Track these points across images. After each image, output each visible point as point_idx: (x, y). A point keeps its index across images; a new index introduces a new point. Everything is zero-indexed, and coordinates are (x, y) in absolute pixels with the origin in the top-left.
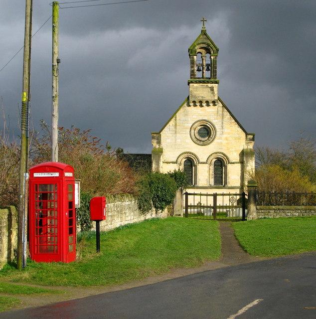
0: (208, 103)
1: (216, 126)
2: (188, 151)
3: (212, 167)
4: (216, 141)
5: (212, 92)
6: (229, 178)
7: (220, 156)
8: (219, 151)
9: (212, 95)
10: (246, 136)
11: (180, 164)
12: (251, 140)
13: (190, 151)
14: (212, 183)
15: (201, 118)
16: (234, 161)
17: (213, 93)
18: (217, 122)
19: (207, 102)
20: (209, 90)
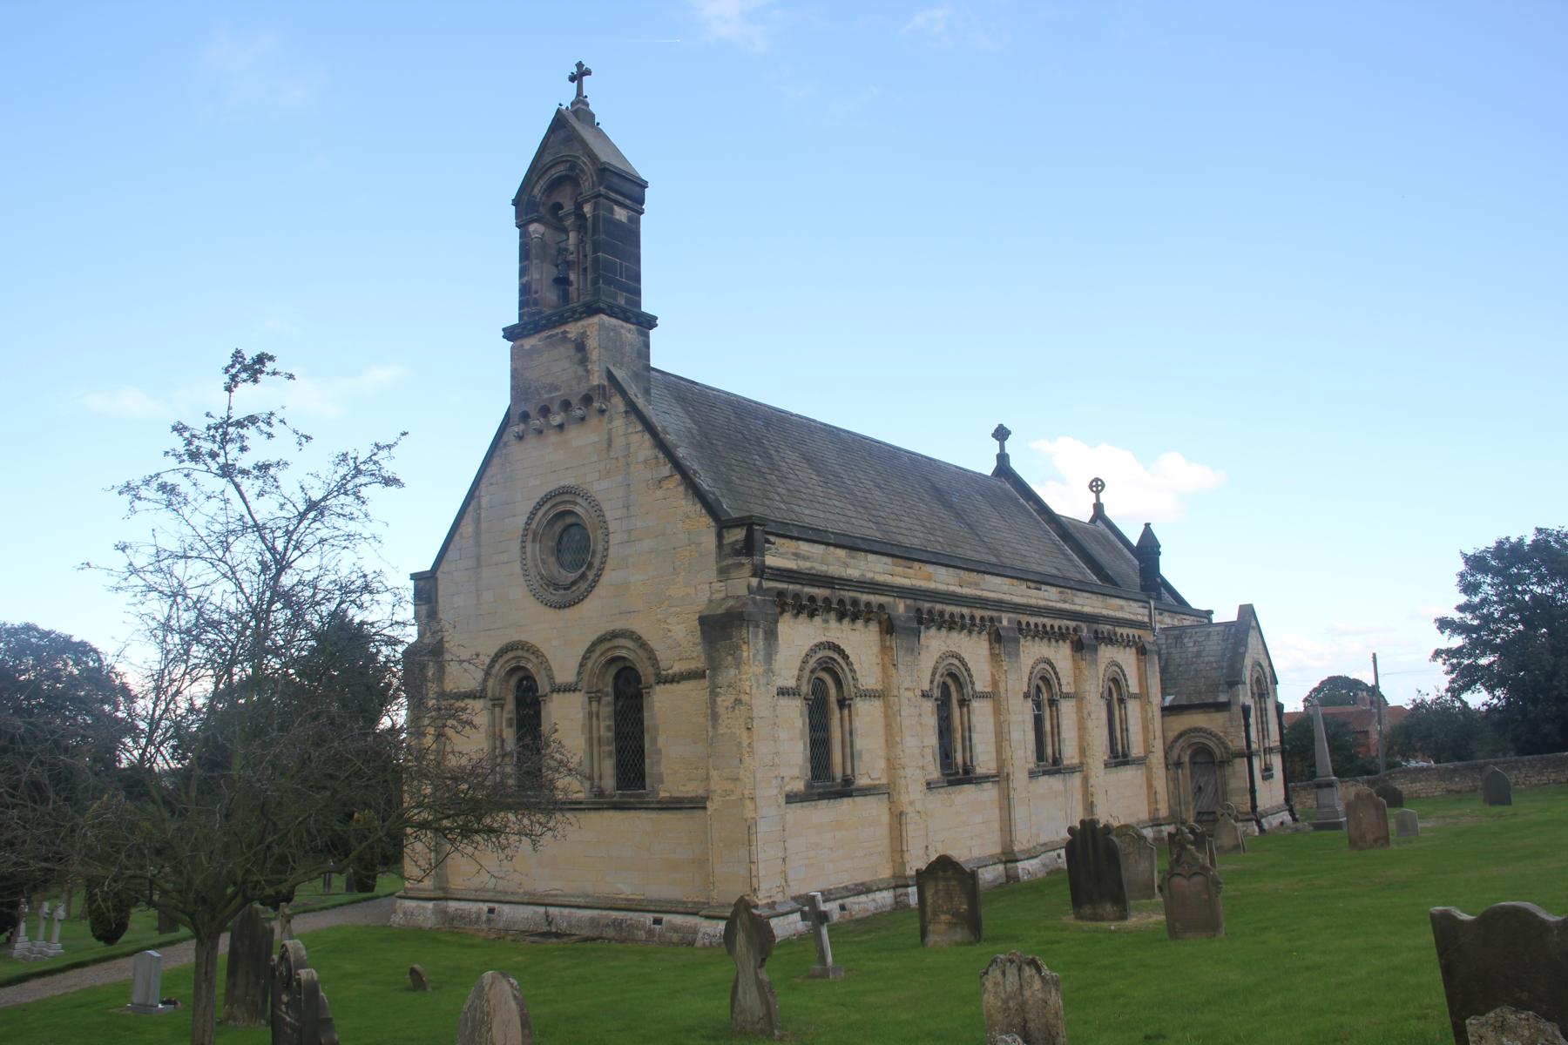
0: (566, 405)
1: (605, 507)
2: (516, 638)
3: (606, 709)
4: (609, 577)
5: (579, 355)
6: (659, 752)
7: (626, 649)
8: (619, 625)
9: (581, 371)
10: (720, 536)
11: (498, 702)
12: (738, 553)
13: (524, 638)
14: (609, 783)
15: (553, 484)
16: (678, 668)
17: (584, 361)
18: (603, 488)
19: (566, 405)
20: (572, 351)
